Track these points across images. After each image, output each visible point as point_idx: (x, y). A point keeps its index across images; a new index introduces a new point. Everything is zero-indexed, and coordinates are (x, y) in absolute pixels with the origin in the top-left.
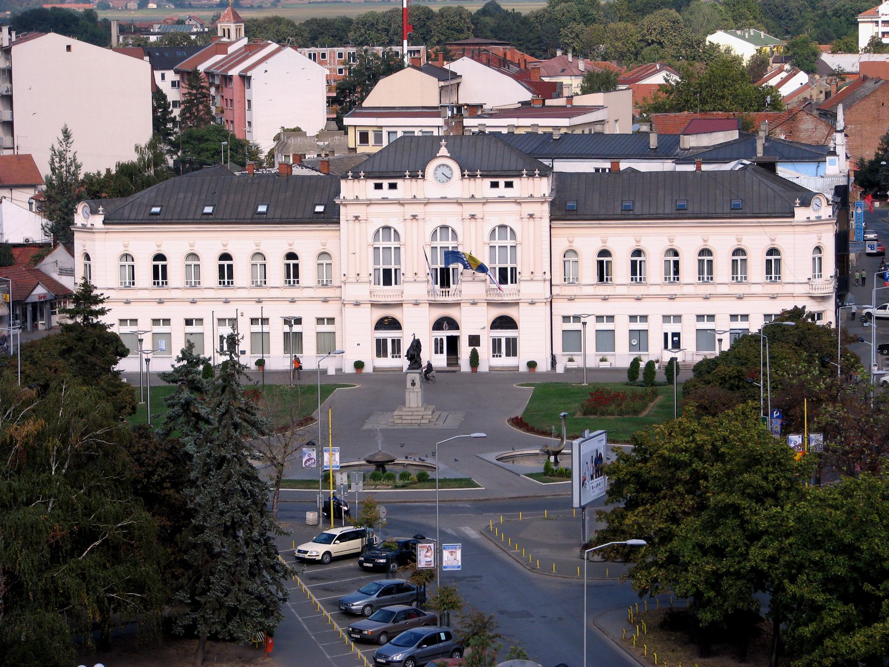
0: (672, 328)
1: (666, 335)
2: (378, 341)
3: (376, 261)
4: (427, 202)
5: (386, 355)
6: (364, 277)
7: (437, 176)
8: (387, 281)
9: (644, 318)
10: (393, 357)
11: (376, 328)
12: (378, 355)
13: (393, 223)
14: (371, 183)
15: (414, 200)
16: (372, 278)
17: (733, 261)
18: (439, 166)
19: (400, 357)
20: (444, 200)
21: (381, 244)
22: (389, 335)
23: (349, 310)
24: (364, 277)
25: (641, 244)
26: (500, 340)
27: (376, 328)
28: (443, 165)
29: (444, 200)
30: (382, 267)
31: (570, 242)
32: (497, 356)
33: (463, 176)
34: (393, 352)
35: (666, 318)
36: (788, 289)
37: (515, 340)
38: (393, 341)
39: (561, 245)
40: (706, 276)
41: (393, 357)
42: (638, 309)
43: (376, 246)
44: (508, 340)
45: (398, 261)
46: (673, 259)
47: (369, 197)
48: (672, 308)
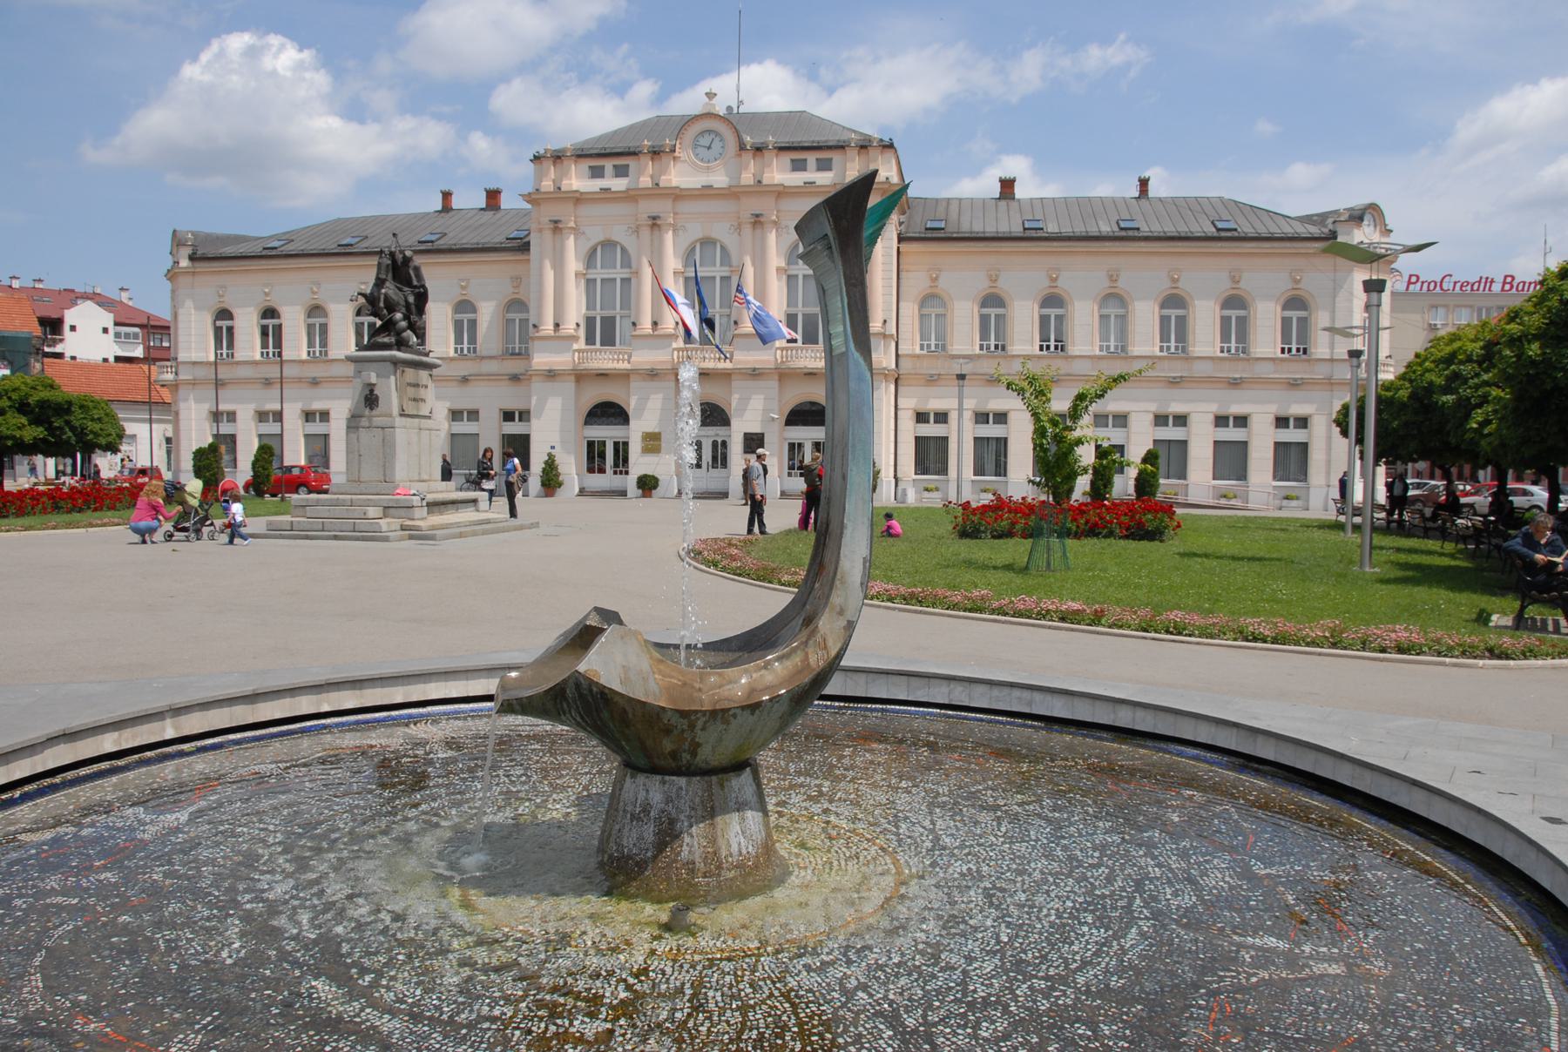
2: (590, 444)
3: (590, 305)
4: (678, 195)
5: (602, 471)
8: (608, 340)
10: (615, 473)
11: (587, 423)
12: (591, 470)
13: (620, 234)
15: (657, 191)
16: (582, 333)
17: (1222, 318)
18: (702, 133)
19: (627, 473)
20: (707, 192)
21: (599, 273)
22: (607, 433)
24: (569, 327)
27: (587, 423)
28: (709, 131)
30: (598, 313)
32: (796, 476)
33: (742, 147)
34: (616, 465)
36: (1320, 372)
38: (616, 444)
40: (1173, 344)
41: (615, 473)
43: (589, 277)
45: (626, 304)
46: (1113, 311)
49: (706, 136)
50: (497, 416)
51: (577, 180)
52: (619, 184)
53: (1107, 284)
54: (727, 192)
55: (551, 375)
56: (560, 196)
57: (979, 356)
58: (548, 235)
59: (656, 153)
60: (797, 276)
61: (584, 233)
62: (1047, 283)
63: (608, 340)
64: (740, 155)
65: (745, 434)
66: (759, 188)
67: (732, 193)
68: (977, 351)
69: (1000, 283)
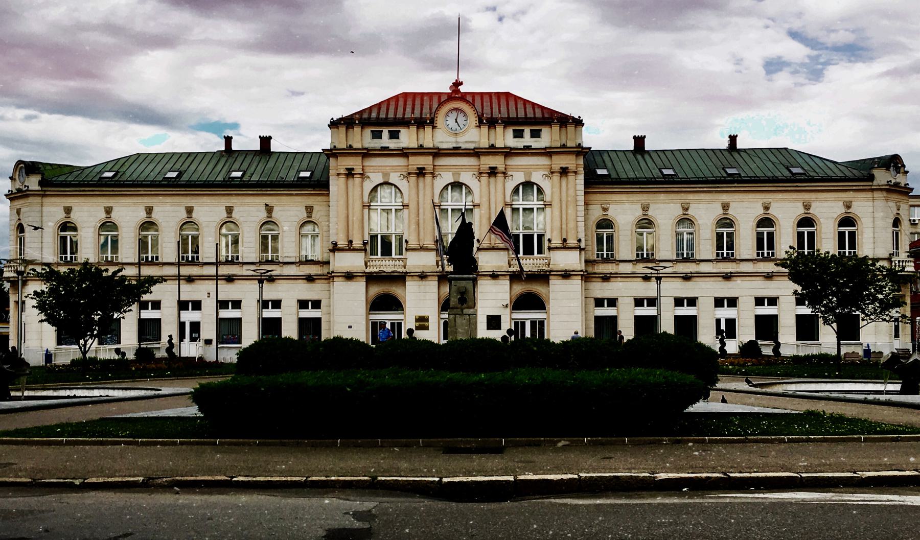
0: (725, 313)
1: (718, 321)
4: (437, 153)
6: (357, 243)
7: (448, 123)
9: (692, 302)
14: (368, 132)
15: (421, 151)
17: (798, 233)
20: (456, 152)
23: (340, 285)
25: (689, 212)
26: (523, 324)
29: (456, 152)
31: (605, 210)
35: (719, 302)
37: (542, 323)
39: (596, 213)
40: (766, 251)
42: (685, 290)
44: (533, 323)
47: (366, 145)
48: (726, 290)
49: (454, 112)
50: (295, 304)
51: (362, 138)
52: (393, 144)
53: (721, 211)
54: (472, 152)
55: (349, 276)
56: (350, 152)
57: (595, 261)
58: (342, 179)
59: (420, 124)
60: (518, 209)
61: (369, 177)
62: (681, 212)
63: (387, 251)
64: (479, 127)
65: (487, 316)
66: (492, 150)
67: (476, 153)
68: (595, 258)
69: (650, 213)
